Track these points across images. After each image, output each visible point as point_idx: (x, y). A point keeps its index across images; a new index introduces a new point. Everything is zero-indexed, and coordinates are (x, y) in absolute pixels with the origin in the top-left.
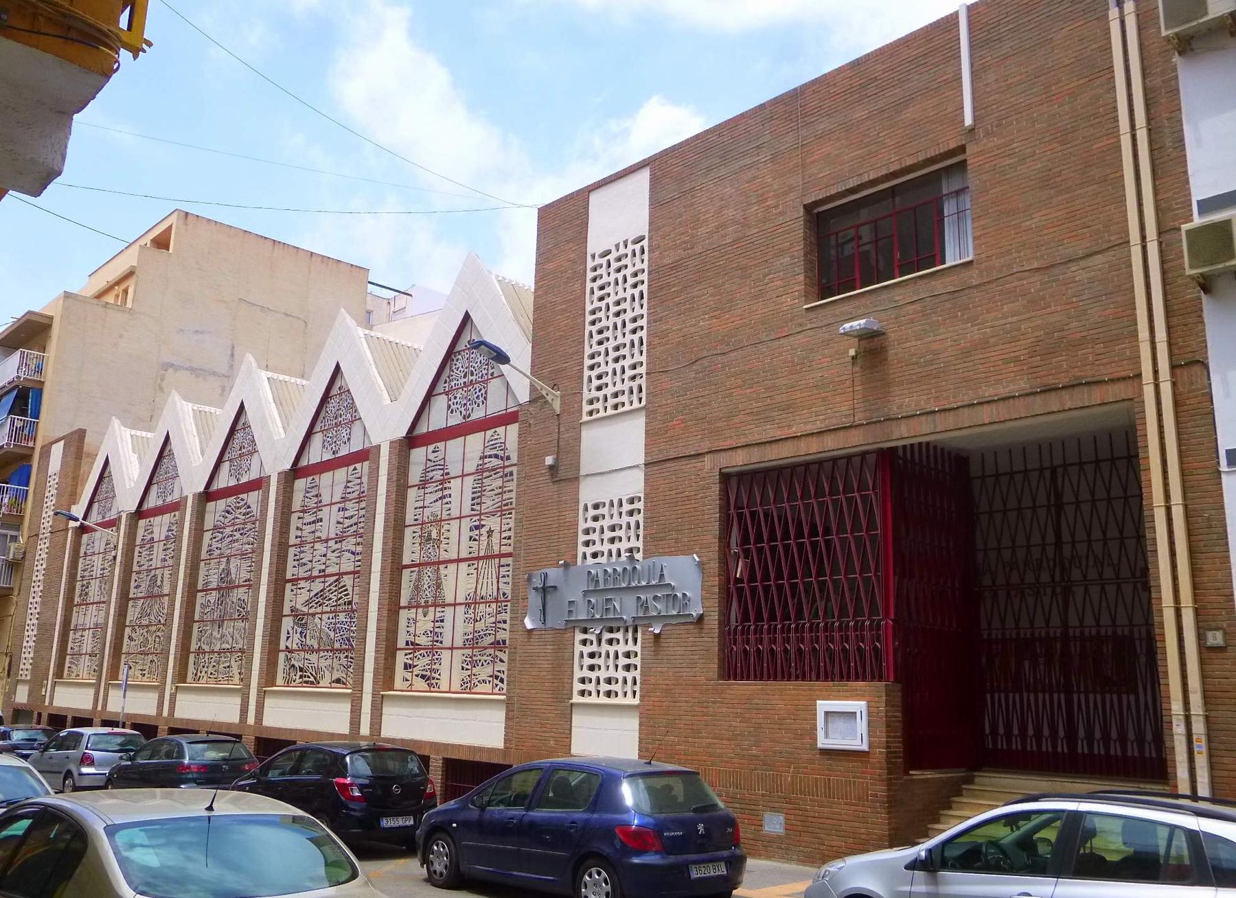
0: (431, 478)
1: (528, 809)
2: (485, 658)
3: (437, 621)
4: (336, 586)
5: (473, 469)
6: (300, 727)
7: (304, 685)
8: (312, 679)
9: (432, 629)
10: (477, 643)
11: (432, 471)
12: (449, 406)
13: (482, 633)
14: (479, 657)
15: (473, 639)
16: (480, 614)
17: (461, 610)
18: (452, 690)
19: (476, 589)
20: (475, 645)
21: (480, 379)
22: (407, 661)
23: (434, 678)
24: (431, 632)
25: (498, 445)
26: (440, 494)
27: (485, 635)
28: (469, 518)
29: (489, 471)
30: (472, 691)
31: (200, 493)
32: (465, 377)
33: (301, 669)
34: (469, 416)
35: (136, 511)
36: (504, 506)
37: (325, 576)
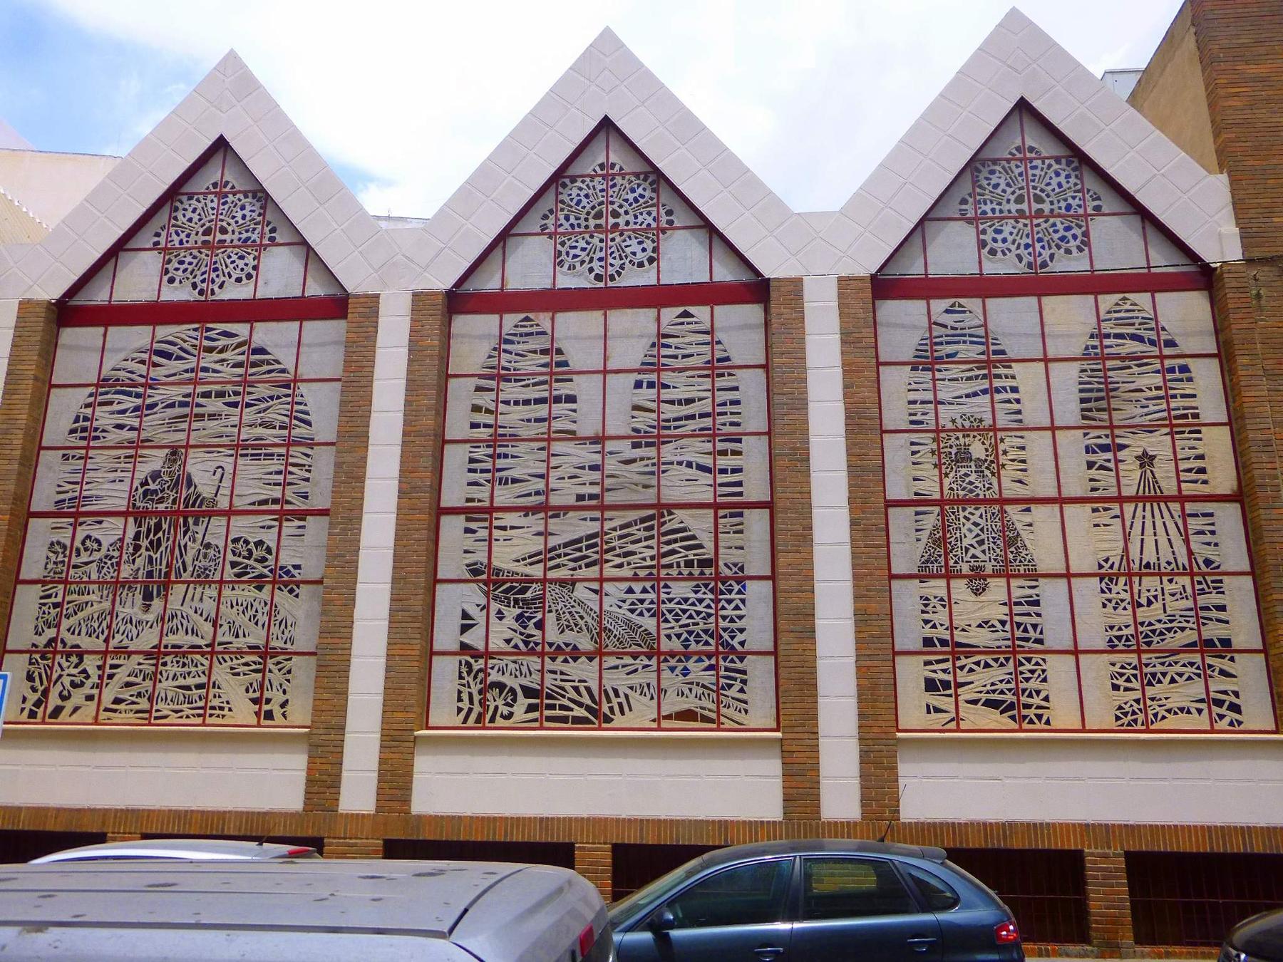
0: (948, 356)
1: (943, 892)
2: (1178, 668)
3: (1017, 604)
4: (646, 529)
5: (634, 359)
6: (583, 812)
7: (546, 724)
8: (579, 712)
9: (1007, 618)
10: (1149, 644)
11: (948, 343)
12: (982, 244)
13: (1158, 626)
14: (1160, 668)
15: (1135, 636)
16: (1145, 594)
17: (1088, 590)
18: (1087, 727)
19: (1126, 549)
20: (1145, 647)
21: (1063, 211)
22: (933, 675)
23: (1028, 706)
24: (1003, 623)
25: (1137, 321)
26: (985, 384)
27: (1169, 630)
28: (1082, 431)
29: (1123, 359)
30: (1152, 727)
31: (49, 303)
32: (205, 234)
33: (529, 693)
34: (1044, 265)
35: (58, 301)
36: (1177, 417)
37: (603, 508)
